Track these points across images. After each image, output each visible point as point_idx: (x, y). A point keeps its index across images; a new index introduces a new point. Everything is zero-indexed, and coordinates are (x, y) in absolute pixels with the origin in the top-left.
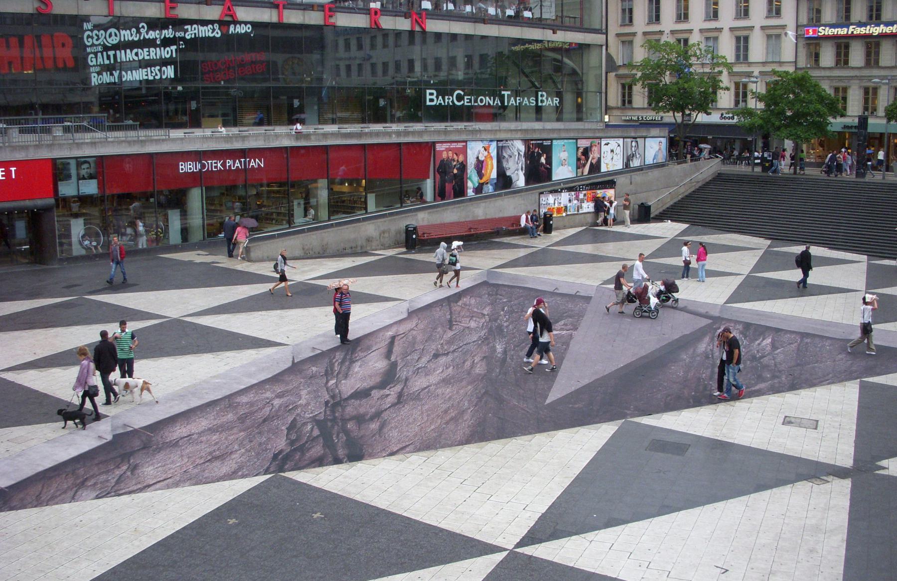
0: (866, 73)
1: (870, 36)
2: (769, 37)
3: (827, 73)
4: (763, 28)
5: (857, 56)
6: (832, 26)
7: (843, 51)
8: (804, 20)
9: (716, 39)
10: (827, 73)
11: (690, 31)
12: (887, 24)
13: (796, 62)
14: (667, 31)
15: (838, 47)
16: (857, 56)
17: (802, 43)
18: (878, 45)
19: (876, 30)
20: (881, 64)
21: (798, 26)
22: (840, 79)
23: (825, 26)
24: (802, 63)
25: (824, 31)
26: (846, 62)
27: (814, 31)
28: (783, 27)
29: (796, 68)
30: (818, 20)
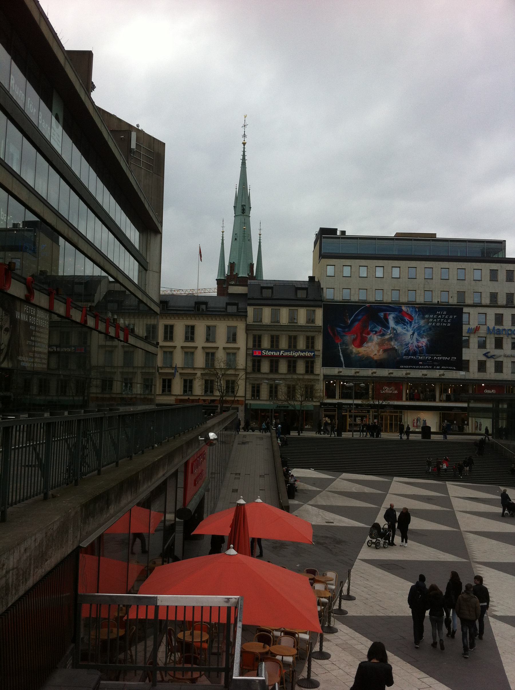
0: (307, 377)
2: (186, 353)
3: (266, 376)
4: (203, 348)
7: (256, 364)
8: (250, 345)
9: (235, 354)
10: (266, 376)
12: (302, 351)
13: (246, 369)
15: (307, 362)
16: (283, 367)
17: (250, 358)
19: (296, 354)
21: (247, 349)
23: (266, 350)
24: (250, 369)
27: (259, 353)
28: (238, 349)
30: (260, 346)
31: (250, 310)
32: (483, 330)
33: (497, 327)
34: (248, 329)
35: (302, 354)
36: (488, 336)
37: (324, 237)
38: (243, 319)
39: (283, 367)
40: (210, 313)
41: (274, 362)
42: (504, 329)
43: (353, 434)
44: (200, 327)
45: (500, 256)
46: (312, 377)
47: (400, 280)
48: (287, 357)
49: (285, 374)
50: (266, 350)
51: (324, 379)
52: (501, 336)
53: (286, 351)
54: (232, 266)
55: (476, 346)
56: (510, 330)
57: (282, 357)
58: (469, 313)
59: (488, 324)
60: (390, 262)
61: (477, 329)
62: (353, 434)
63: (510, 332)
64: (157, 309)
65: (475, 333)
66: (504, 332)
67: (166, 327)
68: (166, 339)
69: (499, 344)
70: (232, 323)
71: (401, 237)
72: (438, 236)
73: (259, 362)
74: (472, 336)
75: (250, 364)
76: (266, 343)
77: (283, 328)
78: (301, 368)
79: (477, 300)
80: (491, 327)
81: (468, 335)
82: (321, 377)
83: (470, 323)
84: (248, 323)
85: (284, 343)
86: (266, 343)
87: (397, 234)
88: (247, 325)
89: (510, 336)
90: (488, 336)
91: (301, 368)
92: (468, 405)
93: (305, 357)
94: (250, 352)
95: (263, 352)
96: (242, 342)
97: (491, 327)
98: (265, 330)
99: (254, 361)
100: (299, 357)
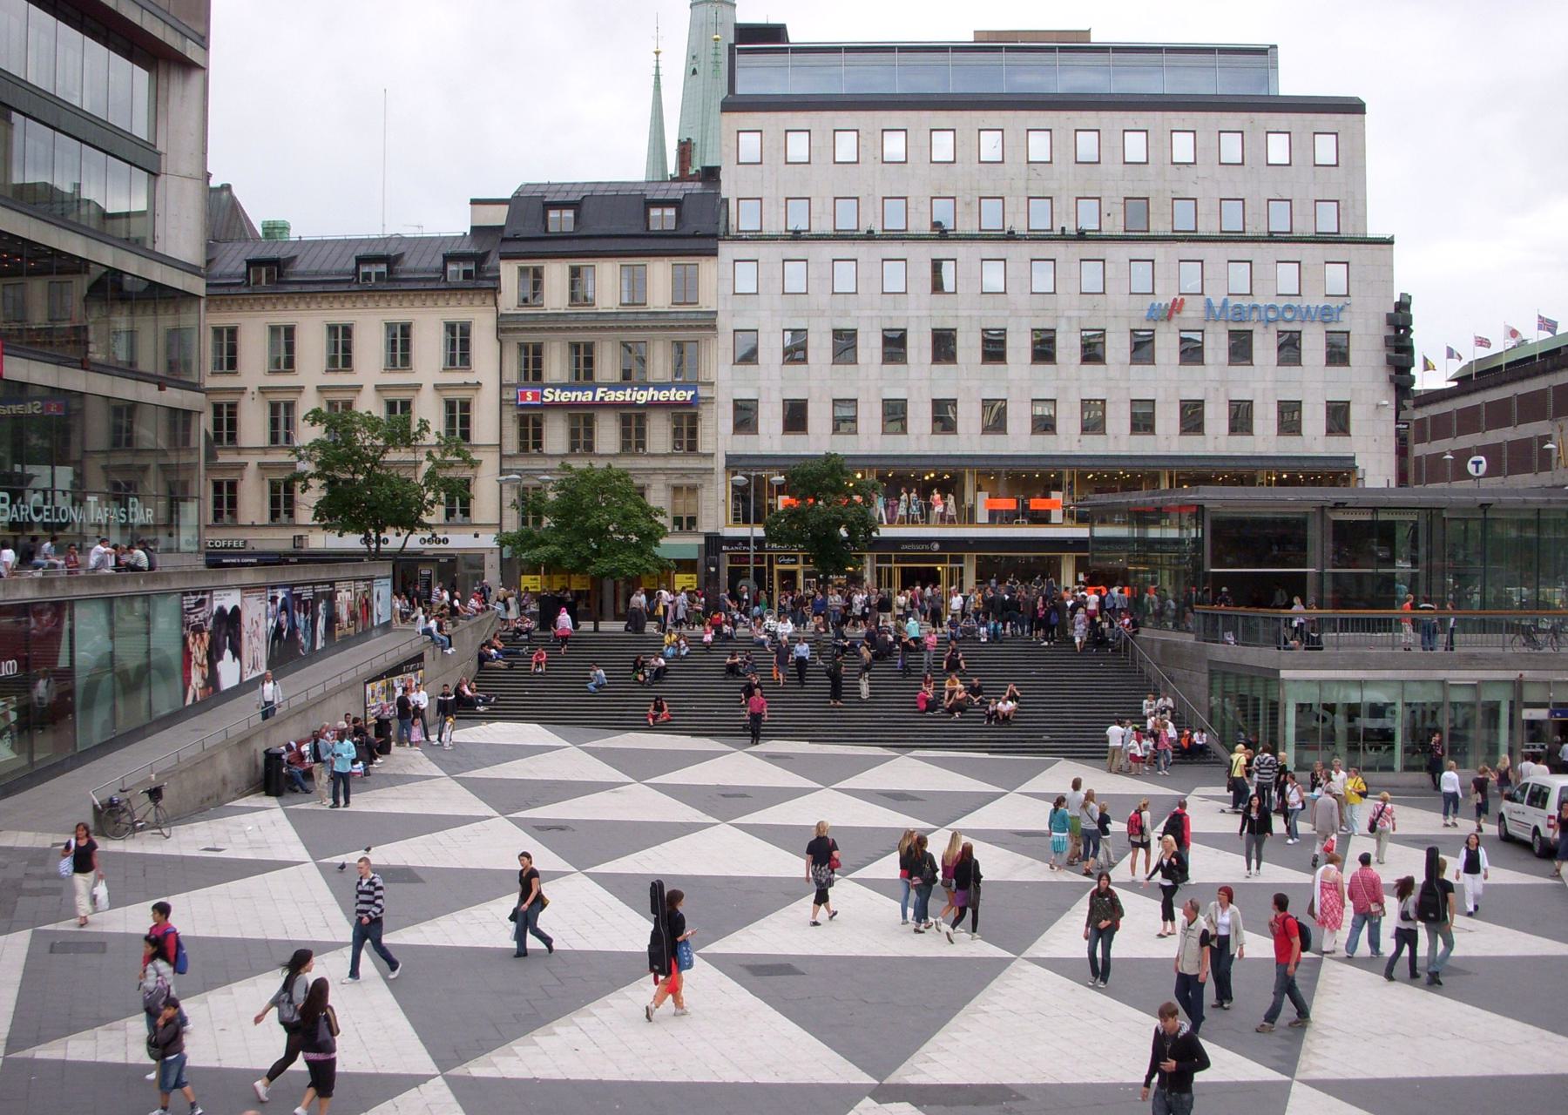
1: (633, 405)
5: (659, 435)
6: (564, 387)
8: (513, 373)
11: (358, 389)
12: (659, 387)
13: (500, 445)
14: (252, 387)
17: (510, 415)
18: (641, 419)
19: (642, 397)
20: (650, 449)
21: (502, 386)
22: (683, 472)
23: (555, 386)
24: (512, 446)
25: (549, 396)
26: (642, 444)
27: (535, 396)
29: (502, 457)
30: (538, 375)
31: (509, 273)
32: (1193, 312)
34: (504, 327)
35: (662, 396)
36: (1209, 327)
37: (741, 51)
38: (490, 301)
39: (556, 437)
40: (405, 286)
41: (582, 420)
42: (1255, 307)
44: (370, 326)
46: (692, 463)
47: (1102, 166)
48: (614, 406)
49: (665, 456)
50: (555, 386)
51: (727, 467)
53: (613, 387)
54: (685, 149)
56: (1272, 307)
57: (603, 405)
59: (1208, 294)
61: (1176, 307)
63: (1271, 315)
64: (197, 286)
65: (1169, 318)
66: (1255, 315)
67: (218, 332)
68: (218, 369)
69: (1241, 348)
70: (458, 312)
71: (990, 45)
73: (538, 424)
75: (512, 432)
76: (556, 365)
77: (555, 323)
78: (607, 436)
80: (1217, 302)
82: (720, 463)
84: (502, 310)
85: (607, 365)
86: (556, 365)
88: (501, 318)
89: (1273, 329)
90: (1209, 327)
91: (607, 436)
93: (668, 405)
94: (511, 395)
95: (546, 392)
96: (488, 363)
97: (1217, 302)
98: (551, 329)
99: (523, 421)
100: (653, 405)
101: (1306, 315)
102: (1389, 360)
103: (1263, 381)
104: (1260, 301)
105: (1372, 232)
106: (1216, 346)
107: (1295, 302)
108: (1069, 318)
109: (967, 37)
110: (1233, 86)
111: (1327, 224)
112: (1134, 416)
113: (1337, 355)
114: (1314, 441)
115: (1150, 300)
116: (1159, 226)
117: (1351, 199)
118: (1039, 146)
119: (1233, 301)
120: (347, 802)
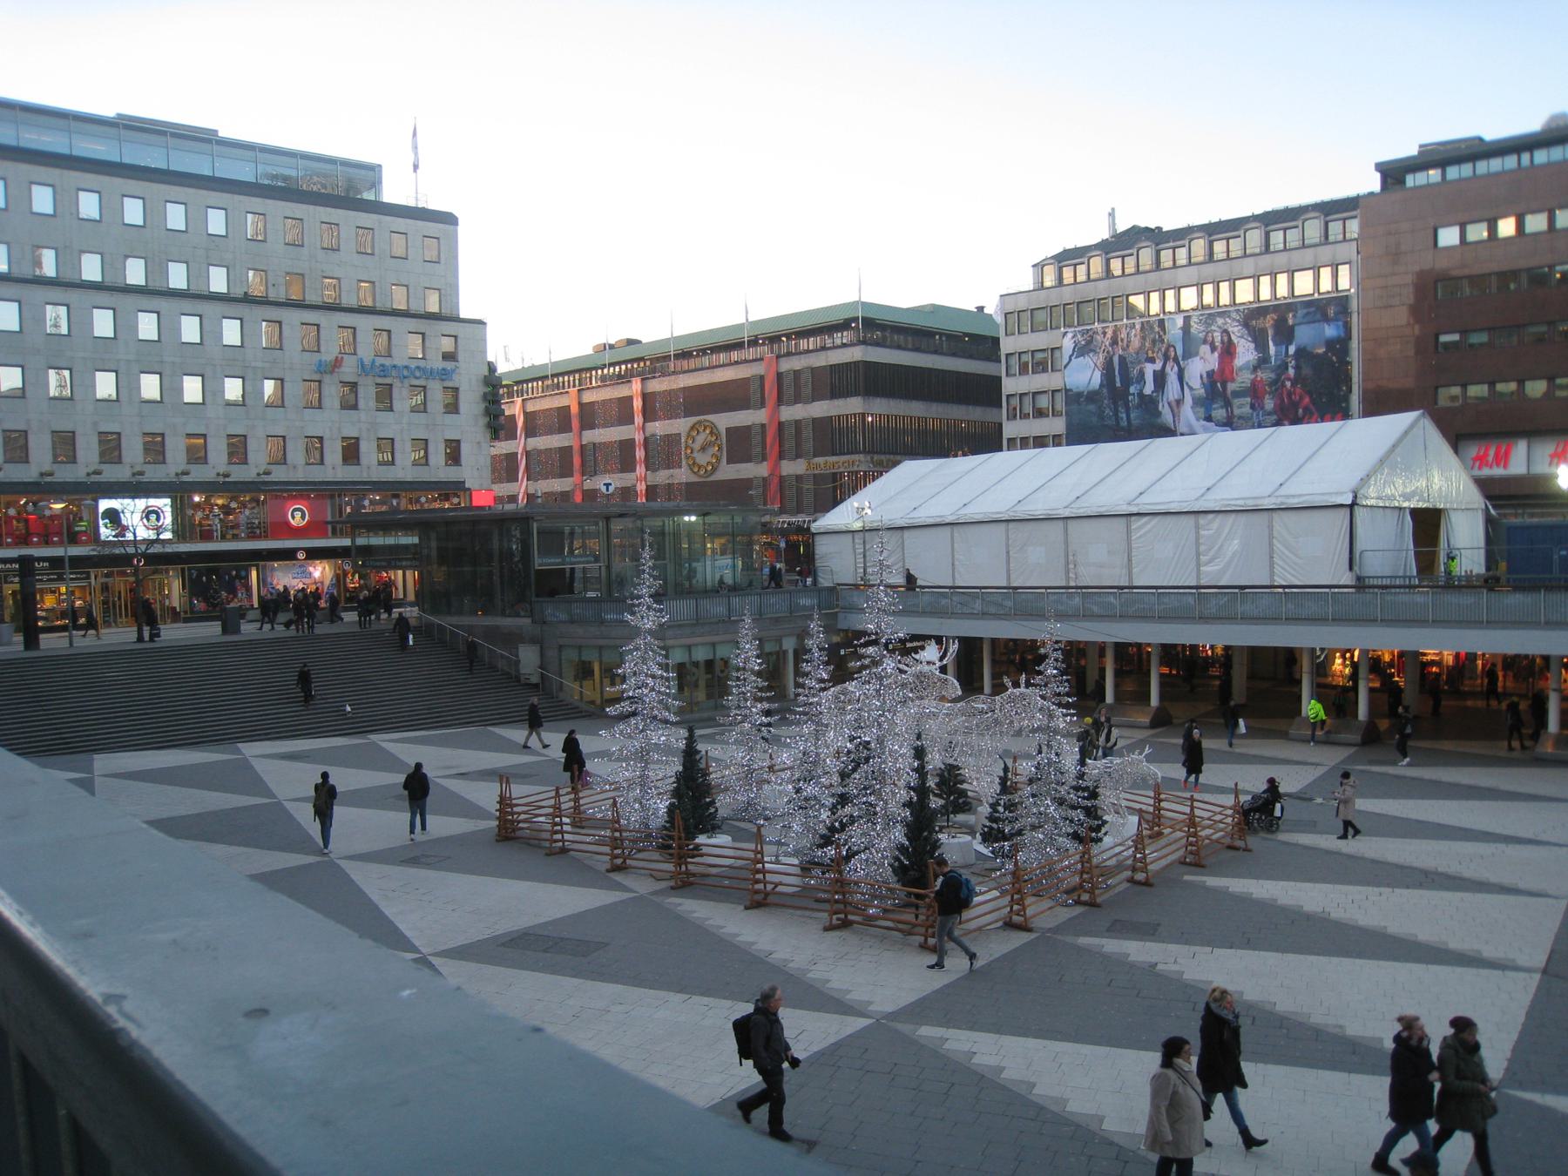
32: (349, 370)
33: (380, 361)
43: (71, 637)
45: (369, 196)
52: (387, 381)
55: (337, 404)
58: (280, 323)
59: (359, 352)
60: (118, 181)
61: (337, 363)
62: (71, 637)
65: (332, 372)
69: (385, 398)
72: (224, 133)
74: (327, 379)
79: (329, 296)
80: (367, 361)
81: (316, 377)
83: (323, 349)
87: (120, 116)
90: (361, 381)
92: (353, 541)
101: (430, 374)
102: (487, 409)
103: (400, 424)
104: (398, 362)
105: (462, 316)
106: (367, 394)
107: (422, 364)
108: (255, 368)
109: (108, 111)
110: (341, 190)
111: (433, 306)
112: (145, 444)
113: (453, 408)
114: (439, 470)
115: (316, 357)
116: (312, 298)
117: (449, 291)
118: (216, 222)
119: (380, 361)
120: (424, 827)
